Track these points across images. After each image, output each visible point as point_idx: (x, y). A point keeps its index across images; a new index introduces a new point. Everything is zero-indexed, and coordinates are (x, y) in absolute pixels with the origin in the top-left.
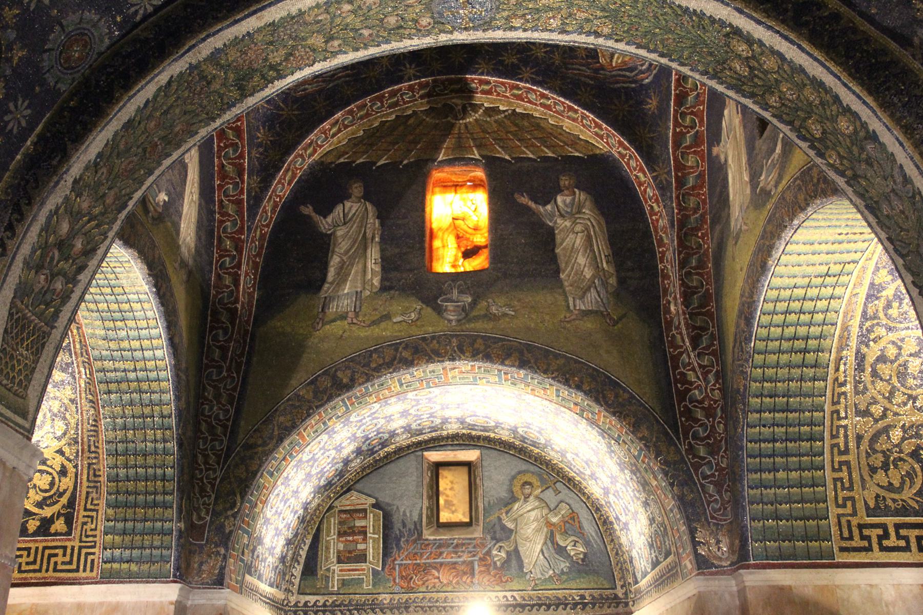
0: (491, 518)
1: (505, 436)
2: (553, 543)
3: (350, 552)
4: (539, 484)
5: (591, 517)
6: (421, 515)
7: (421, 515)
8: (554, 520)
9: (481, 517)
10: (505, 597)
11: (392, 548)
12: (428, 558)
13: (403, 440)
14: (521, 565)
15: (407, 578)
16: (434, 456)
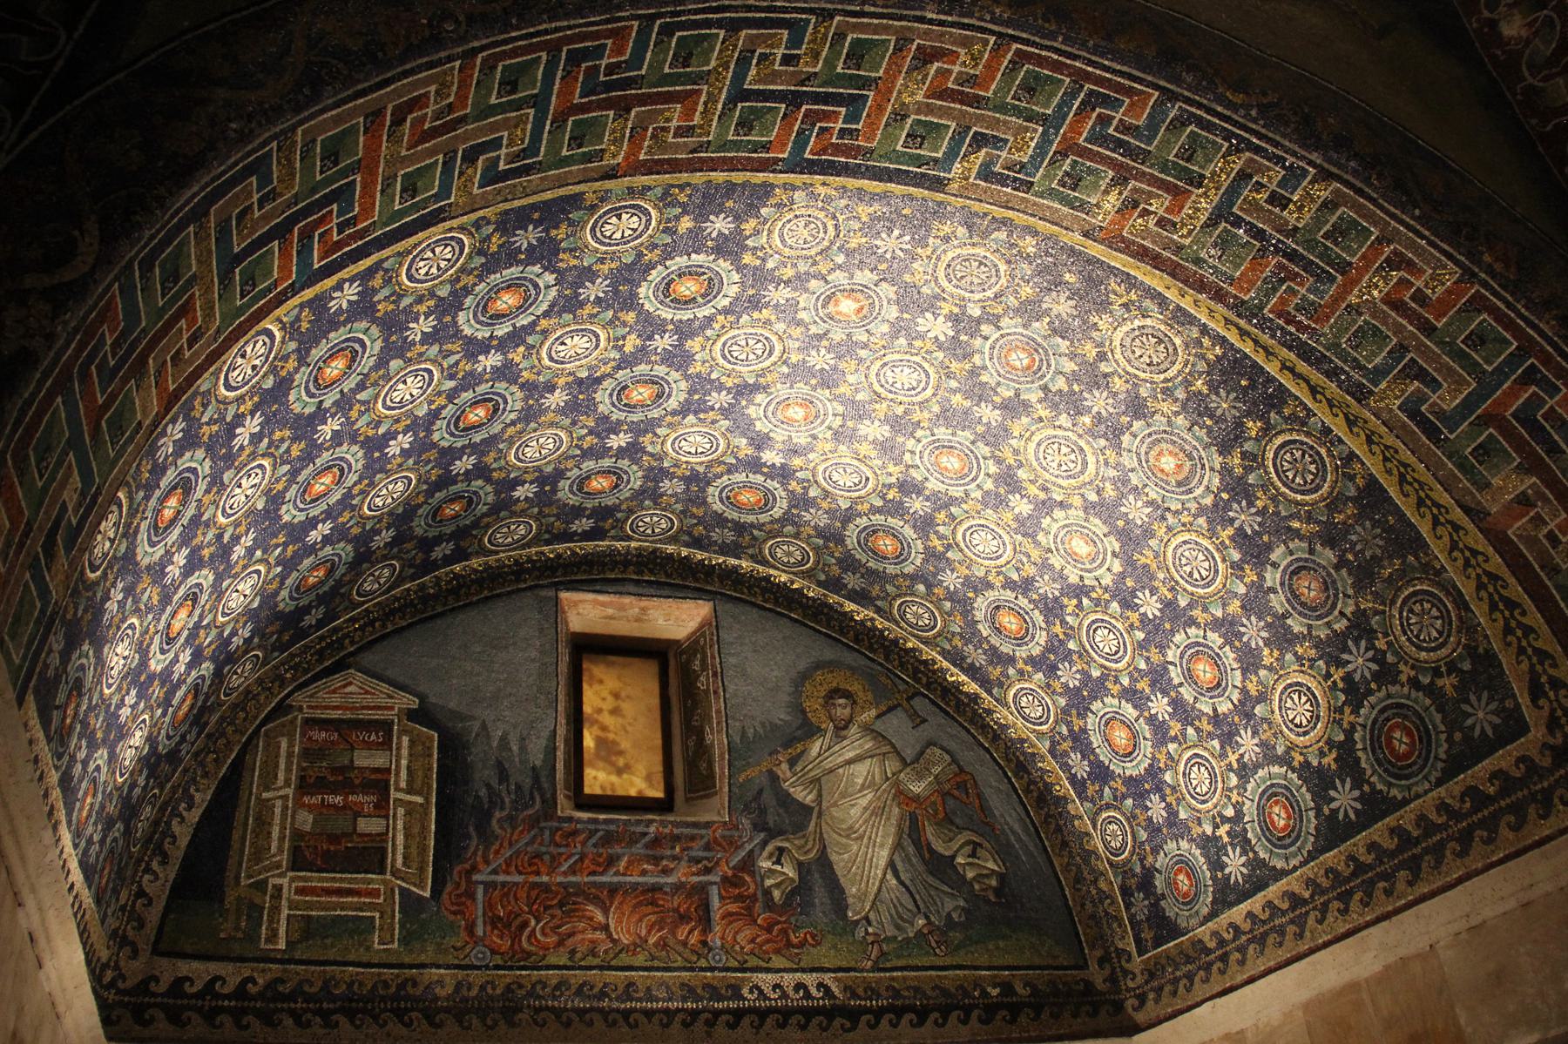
0: (752, 772)
1: (784, 564)
2: (917, 843)
3: (334, 839)
4: (870, 696)
5: (1005, 787)
6: (551, 750)
7: (551, 750)
8: (917, 788)
9: (721, 769)
10: (799, 986)
11: (468, 837)
12: (573, 871)
13: (511, 538)
14: (839, 900)
15: (511, 925)
16: (588, 611)
